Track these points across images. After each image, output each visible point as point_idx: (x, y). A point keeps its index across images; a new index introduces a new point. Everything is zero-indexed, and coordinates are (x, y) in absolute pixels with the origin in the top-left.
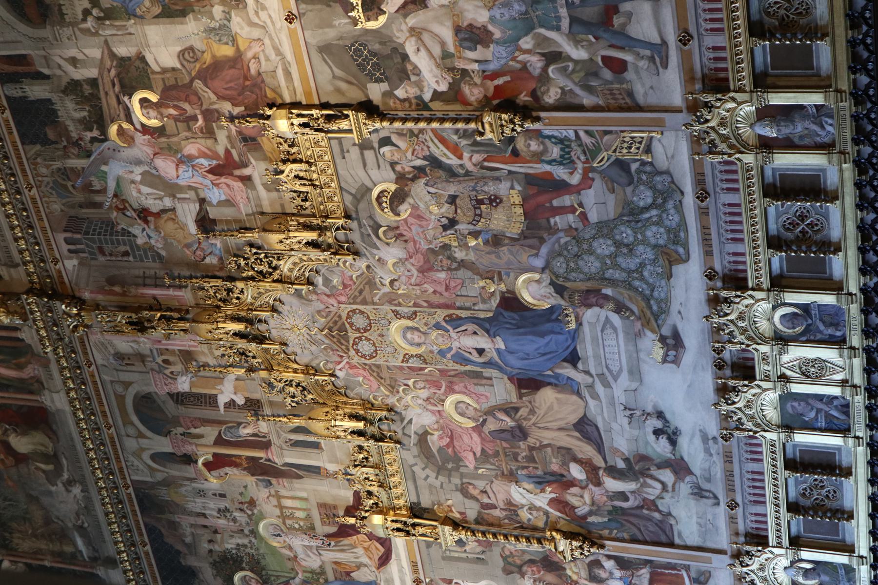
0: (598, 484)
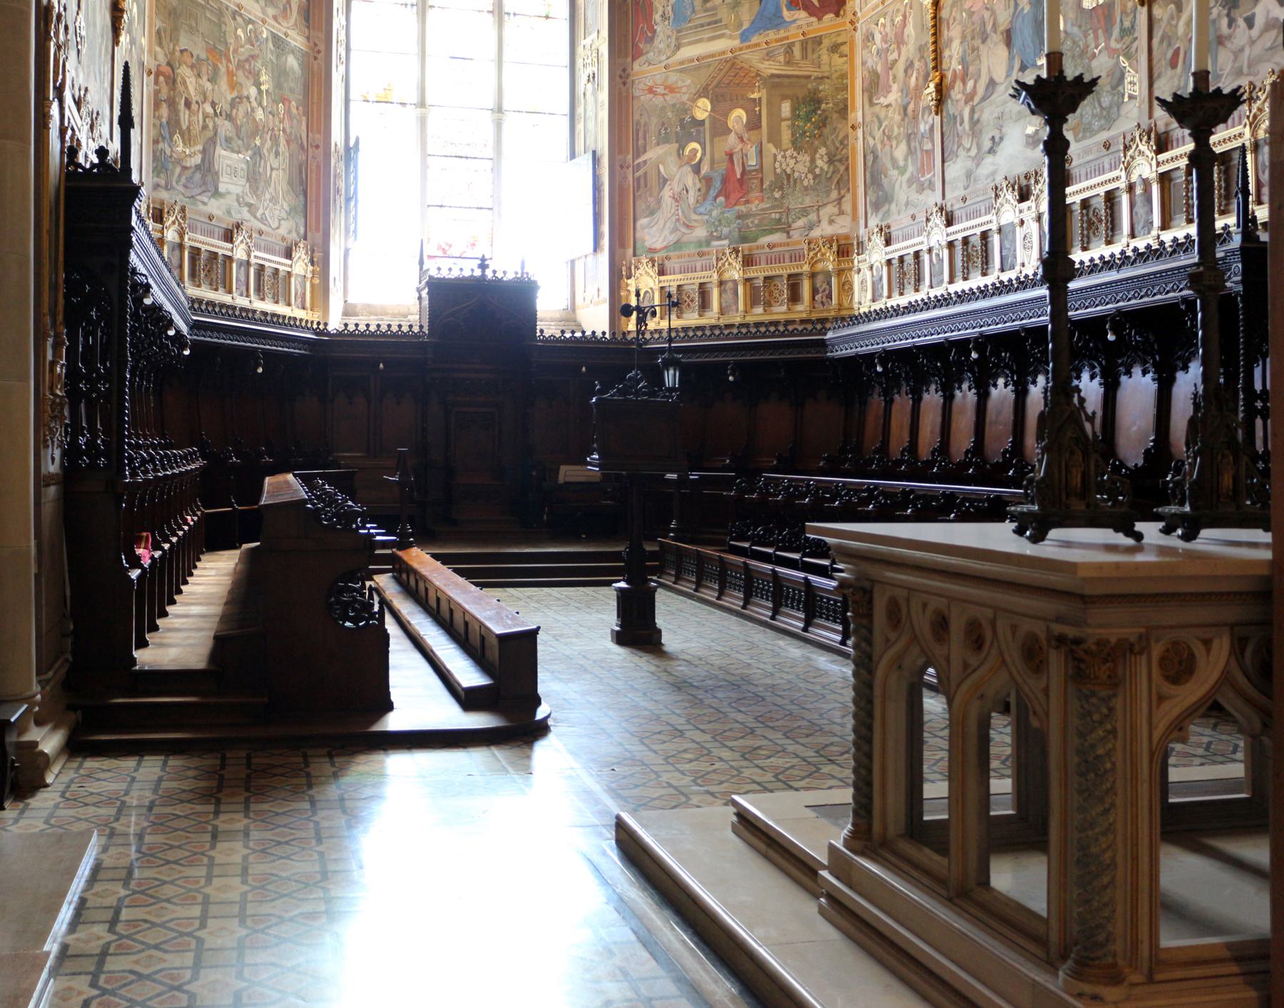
0: (966, 102)
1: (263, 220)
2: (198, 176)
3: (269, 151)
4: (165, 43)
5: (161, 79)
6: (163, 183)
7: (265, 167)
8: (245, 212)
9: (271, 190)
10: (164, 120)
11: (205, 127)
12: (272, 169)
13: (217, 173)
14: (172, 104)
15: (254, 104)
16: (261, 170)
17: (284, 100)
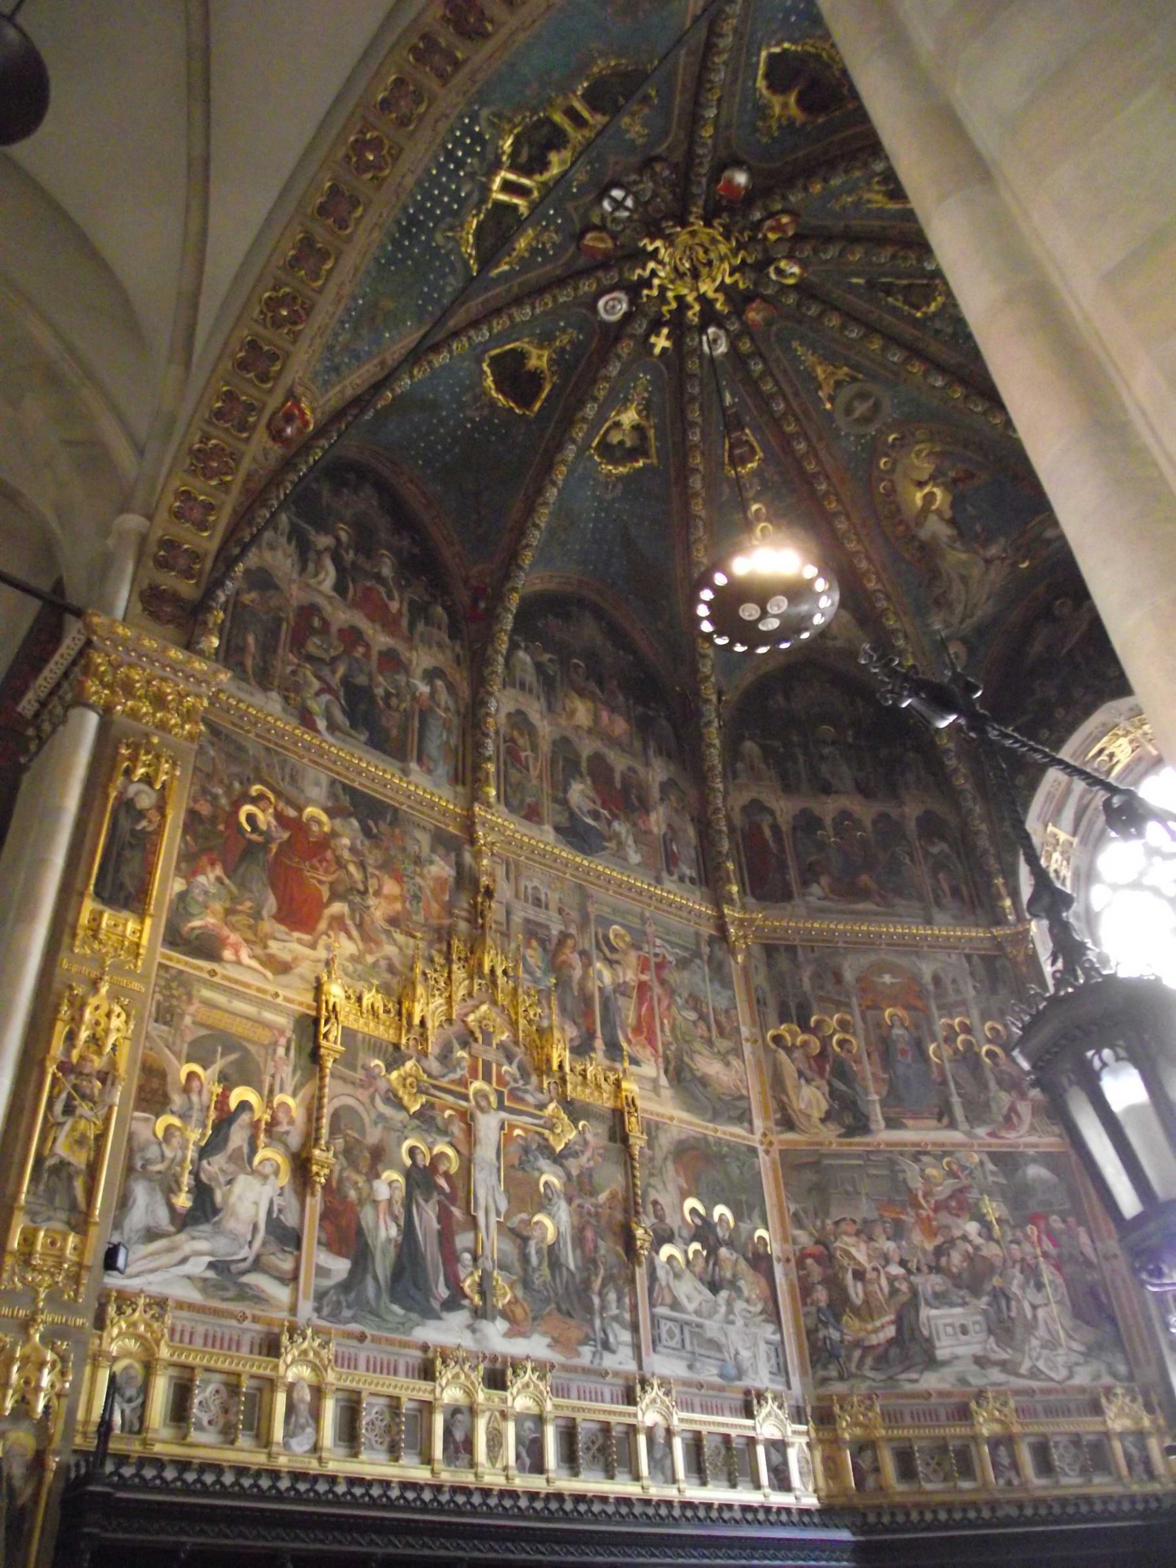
1: (1035, 1373)
2: (894, 1352)
3: (1023, 1287)
4: (806, 1222)
5: (809, 1261)
6: (834, 1373)
7: (1021, 1309)
8: (996, 1375)
9: (1041, 1332)
10: (823, 1304)
11: (894, 1292)
12: (1034, 1307)
13: (929, 1340)
14: (834, 1283)
15: (979, 1241)
16: (1013, 1314)
17: (1034, 1219)
